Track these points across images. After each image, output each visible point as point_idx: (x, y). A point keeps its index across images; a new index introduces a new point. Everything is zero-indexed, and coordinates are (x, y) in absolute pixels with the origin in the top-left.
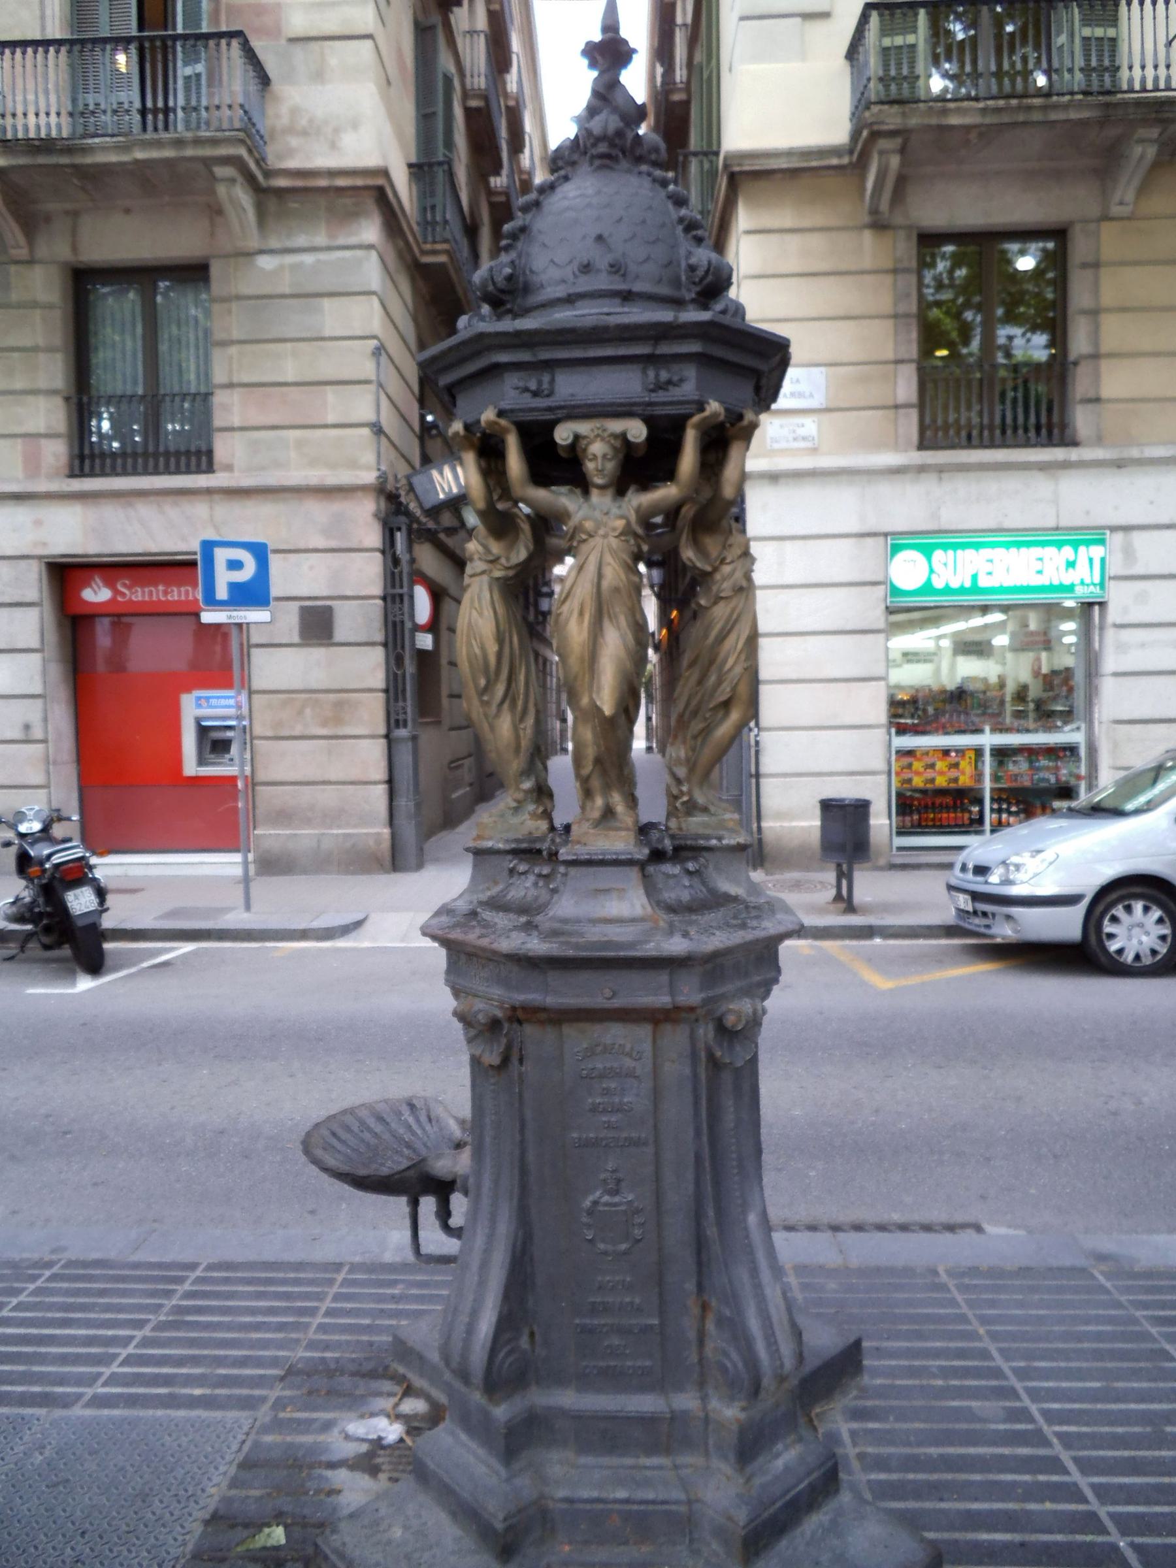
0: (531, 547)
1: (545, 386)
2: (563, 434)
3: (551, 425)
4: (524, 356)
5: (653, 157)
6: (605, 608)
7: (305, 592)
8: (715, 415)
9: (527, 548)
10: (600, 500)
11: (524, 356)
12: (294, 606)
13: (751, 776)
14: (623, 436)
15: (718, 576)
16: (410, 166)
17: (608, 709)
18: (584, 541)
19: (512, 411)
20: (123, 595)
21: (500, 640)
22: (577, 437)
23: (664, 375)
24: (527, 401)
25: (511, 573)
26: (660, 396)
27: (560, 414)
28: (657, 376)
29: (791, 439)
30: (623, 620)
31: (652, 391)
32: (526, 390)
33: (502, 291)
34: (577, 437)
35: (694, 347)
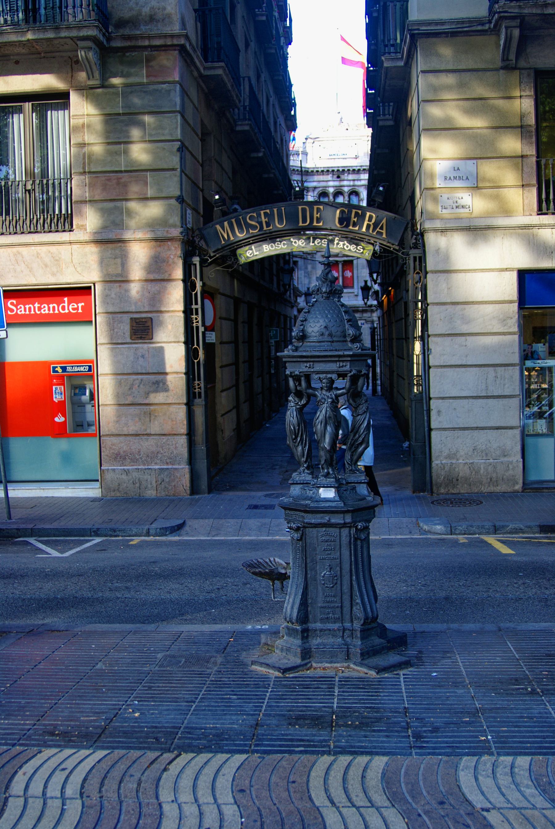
7: (133, 309)
12: (126, 318)
14: (331, 378)
16: (195, 11)
20: (12, 311)
21: (299, 426)
24: (306, 369)
26: (341, 369)
29: (454, 207)
30: (332, 425)
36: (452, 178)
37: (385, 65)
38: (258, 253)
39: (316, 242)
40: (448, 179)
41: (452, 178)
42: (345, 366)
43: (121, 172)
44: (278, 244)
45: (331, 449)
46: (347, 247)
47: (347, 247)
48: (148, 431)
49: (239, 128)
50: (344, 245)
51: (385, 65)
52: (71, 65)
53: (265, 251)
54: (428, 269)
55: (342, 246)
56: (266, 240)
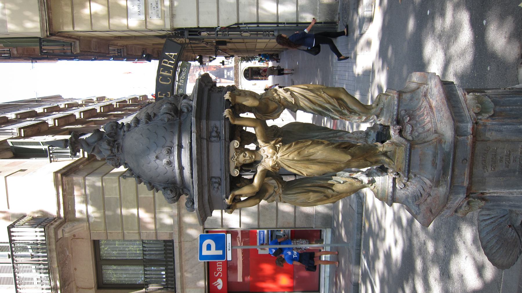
0: (271, 178)
1: (217, 180)
5: (115, 127)
6: (307, 158)
8: (230, 114)
9: (271, 180)
18: (278, 165)
19: (226, 193)
23: (214, 134)
25: (280, 186)
27: (228, 175)
28: (215, 137)
32: (218, 188)
33: (176, 193)
36: (139, 10)
37: (79, 52)
40: (139, 13)
46: (183, 77)
47: (183, 77)
50: (182, 79)
51: (79, 52)
52: (76, 239)
54: (196, 26)
55: (183, 81)
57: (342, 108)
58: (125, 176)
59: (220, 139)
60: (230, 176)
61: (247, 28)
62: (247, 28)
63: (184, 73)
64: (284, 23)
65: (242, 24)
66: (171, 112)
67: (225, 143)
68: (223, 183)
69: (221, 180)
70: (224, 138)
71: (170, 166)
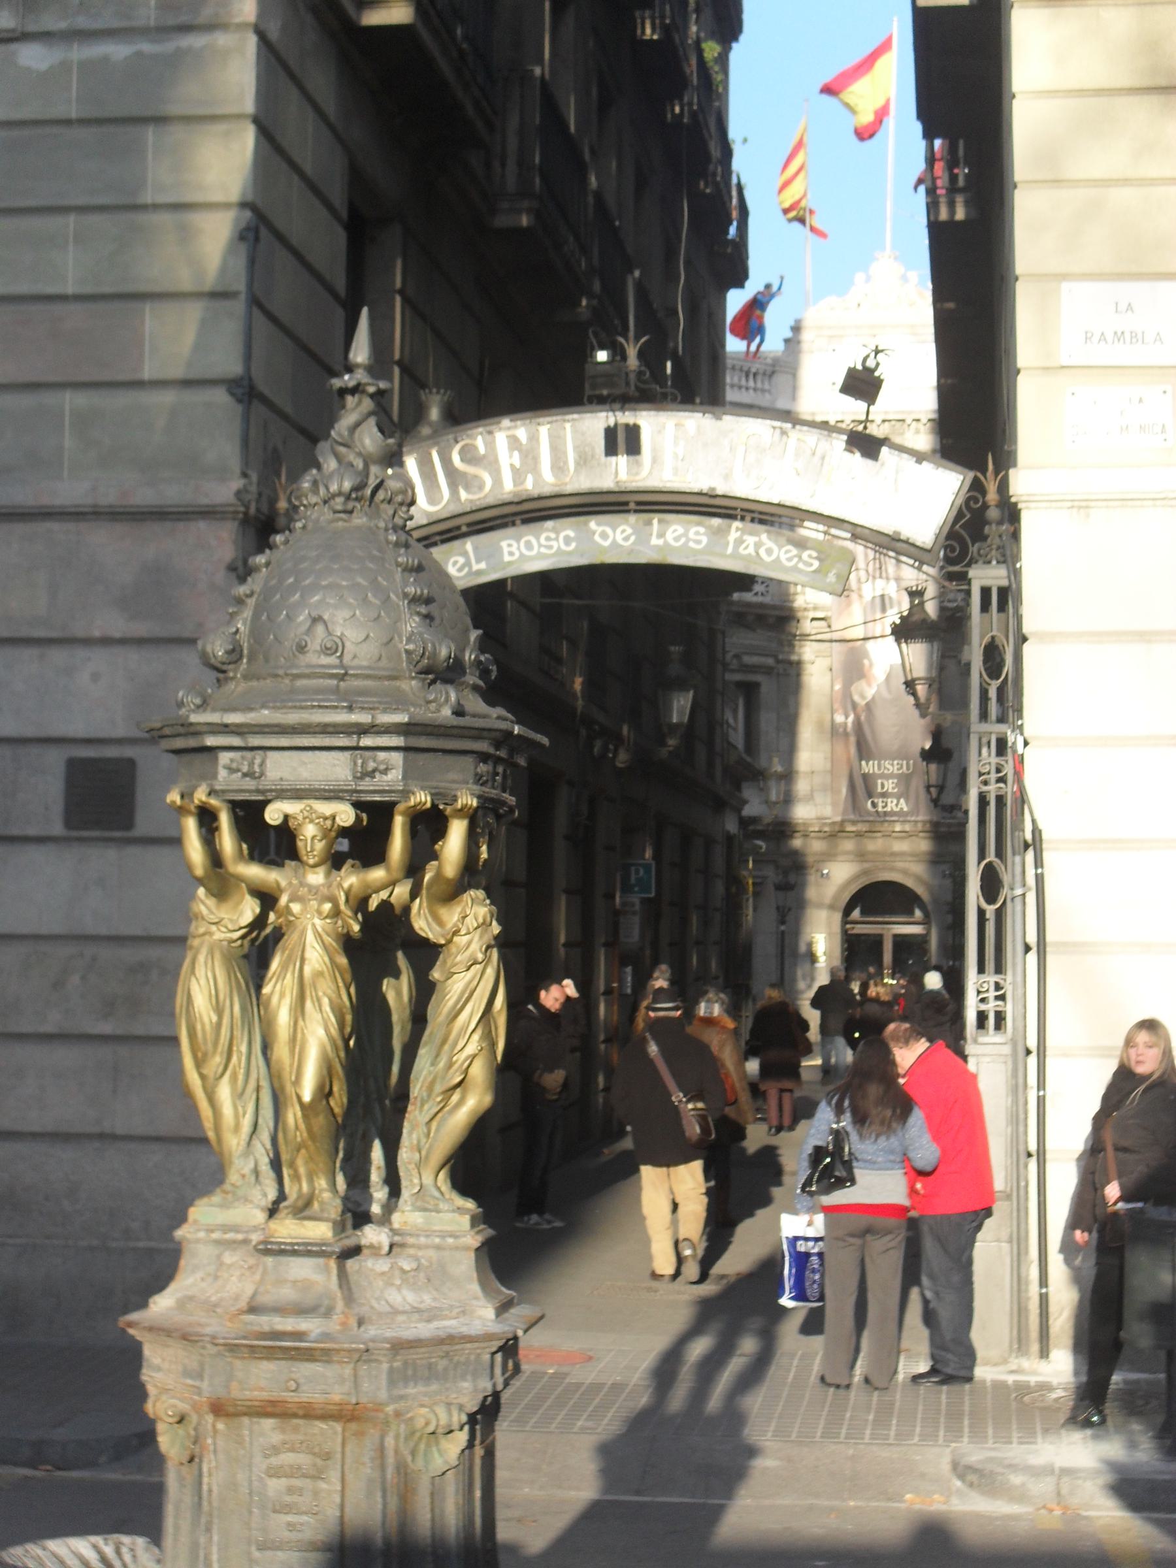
2: (273, 815)
3: (264, 804)
4: (236, 741)
7: (78, 729)
10: (316, 878)
11: (236, 741)
12: (55, 760)
13: (1029, 1155)
15: (454, 949)
17: (307, 1097)
19: (223, 791)
22: (286, 817)
26: (366, 784)
31: (361, 778)
33: (223, 663)
34: (286, 817)
35: (398, 741)
36: (1110, 336)
38: (483, 566)
39: (670, 536)
40: (1096, 339)
41: (1110, 336)
42: (385, 772)
43: (63, 298)
44: (548, 539)
45: (314, 1100)
47: (769, 552)
48: (107, 1127)
49: (502, 221)
50: (758, 545)
53: (507, 558)
55: (751, 550)
56: (514, 524)
57: (439, 1099)
58: (257, 239)
59: (358, 778)
60: (266, 803)
61: (1019, 891)
62: (1019, 891)
63: (790, 559)
64: (1041, 1084)
65: (1039, 862)
66: (428, 659)
67: (346, 791)
68: (249, 784)
69: (255, 778)
70: (358, 788)
71: (294, 648)
